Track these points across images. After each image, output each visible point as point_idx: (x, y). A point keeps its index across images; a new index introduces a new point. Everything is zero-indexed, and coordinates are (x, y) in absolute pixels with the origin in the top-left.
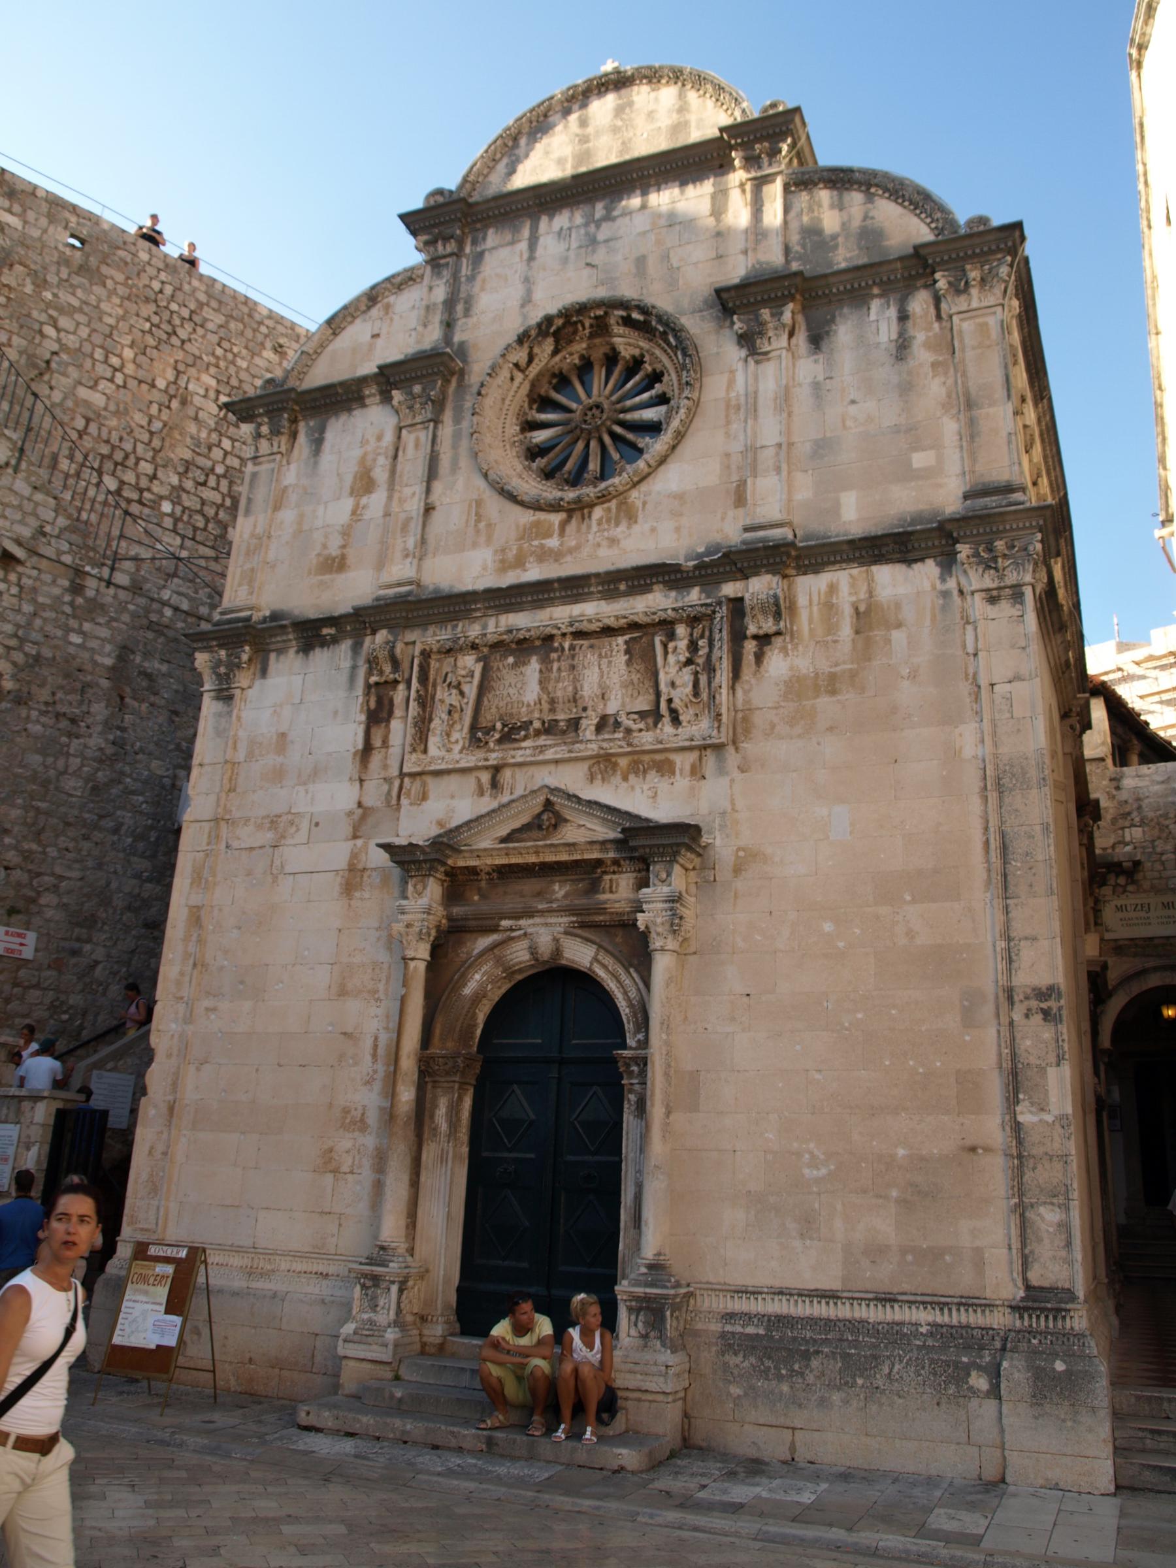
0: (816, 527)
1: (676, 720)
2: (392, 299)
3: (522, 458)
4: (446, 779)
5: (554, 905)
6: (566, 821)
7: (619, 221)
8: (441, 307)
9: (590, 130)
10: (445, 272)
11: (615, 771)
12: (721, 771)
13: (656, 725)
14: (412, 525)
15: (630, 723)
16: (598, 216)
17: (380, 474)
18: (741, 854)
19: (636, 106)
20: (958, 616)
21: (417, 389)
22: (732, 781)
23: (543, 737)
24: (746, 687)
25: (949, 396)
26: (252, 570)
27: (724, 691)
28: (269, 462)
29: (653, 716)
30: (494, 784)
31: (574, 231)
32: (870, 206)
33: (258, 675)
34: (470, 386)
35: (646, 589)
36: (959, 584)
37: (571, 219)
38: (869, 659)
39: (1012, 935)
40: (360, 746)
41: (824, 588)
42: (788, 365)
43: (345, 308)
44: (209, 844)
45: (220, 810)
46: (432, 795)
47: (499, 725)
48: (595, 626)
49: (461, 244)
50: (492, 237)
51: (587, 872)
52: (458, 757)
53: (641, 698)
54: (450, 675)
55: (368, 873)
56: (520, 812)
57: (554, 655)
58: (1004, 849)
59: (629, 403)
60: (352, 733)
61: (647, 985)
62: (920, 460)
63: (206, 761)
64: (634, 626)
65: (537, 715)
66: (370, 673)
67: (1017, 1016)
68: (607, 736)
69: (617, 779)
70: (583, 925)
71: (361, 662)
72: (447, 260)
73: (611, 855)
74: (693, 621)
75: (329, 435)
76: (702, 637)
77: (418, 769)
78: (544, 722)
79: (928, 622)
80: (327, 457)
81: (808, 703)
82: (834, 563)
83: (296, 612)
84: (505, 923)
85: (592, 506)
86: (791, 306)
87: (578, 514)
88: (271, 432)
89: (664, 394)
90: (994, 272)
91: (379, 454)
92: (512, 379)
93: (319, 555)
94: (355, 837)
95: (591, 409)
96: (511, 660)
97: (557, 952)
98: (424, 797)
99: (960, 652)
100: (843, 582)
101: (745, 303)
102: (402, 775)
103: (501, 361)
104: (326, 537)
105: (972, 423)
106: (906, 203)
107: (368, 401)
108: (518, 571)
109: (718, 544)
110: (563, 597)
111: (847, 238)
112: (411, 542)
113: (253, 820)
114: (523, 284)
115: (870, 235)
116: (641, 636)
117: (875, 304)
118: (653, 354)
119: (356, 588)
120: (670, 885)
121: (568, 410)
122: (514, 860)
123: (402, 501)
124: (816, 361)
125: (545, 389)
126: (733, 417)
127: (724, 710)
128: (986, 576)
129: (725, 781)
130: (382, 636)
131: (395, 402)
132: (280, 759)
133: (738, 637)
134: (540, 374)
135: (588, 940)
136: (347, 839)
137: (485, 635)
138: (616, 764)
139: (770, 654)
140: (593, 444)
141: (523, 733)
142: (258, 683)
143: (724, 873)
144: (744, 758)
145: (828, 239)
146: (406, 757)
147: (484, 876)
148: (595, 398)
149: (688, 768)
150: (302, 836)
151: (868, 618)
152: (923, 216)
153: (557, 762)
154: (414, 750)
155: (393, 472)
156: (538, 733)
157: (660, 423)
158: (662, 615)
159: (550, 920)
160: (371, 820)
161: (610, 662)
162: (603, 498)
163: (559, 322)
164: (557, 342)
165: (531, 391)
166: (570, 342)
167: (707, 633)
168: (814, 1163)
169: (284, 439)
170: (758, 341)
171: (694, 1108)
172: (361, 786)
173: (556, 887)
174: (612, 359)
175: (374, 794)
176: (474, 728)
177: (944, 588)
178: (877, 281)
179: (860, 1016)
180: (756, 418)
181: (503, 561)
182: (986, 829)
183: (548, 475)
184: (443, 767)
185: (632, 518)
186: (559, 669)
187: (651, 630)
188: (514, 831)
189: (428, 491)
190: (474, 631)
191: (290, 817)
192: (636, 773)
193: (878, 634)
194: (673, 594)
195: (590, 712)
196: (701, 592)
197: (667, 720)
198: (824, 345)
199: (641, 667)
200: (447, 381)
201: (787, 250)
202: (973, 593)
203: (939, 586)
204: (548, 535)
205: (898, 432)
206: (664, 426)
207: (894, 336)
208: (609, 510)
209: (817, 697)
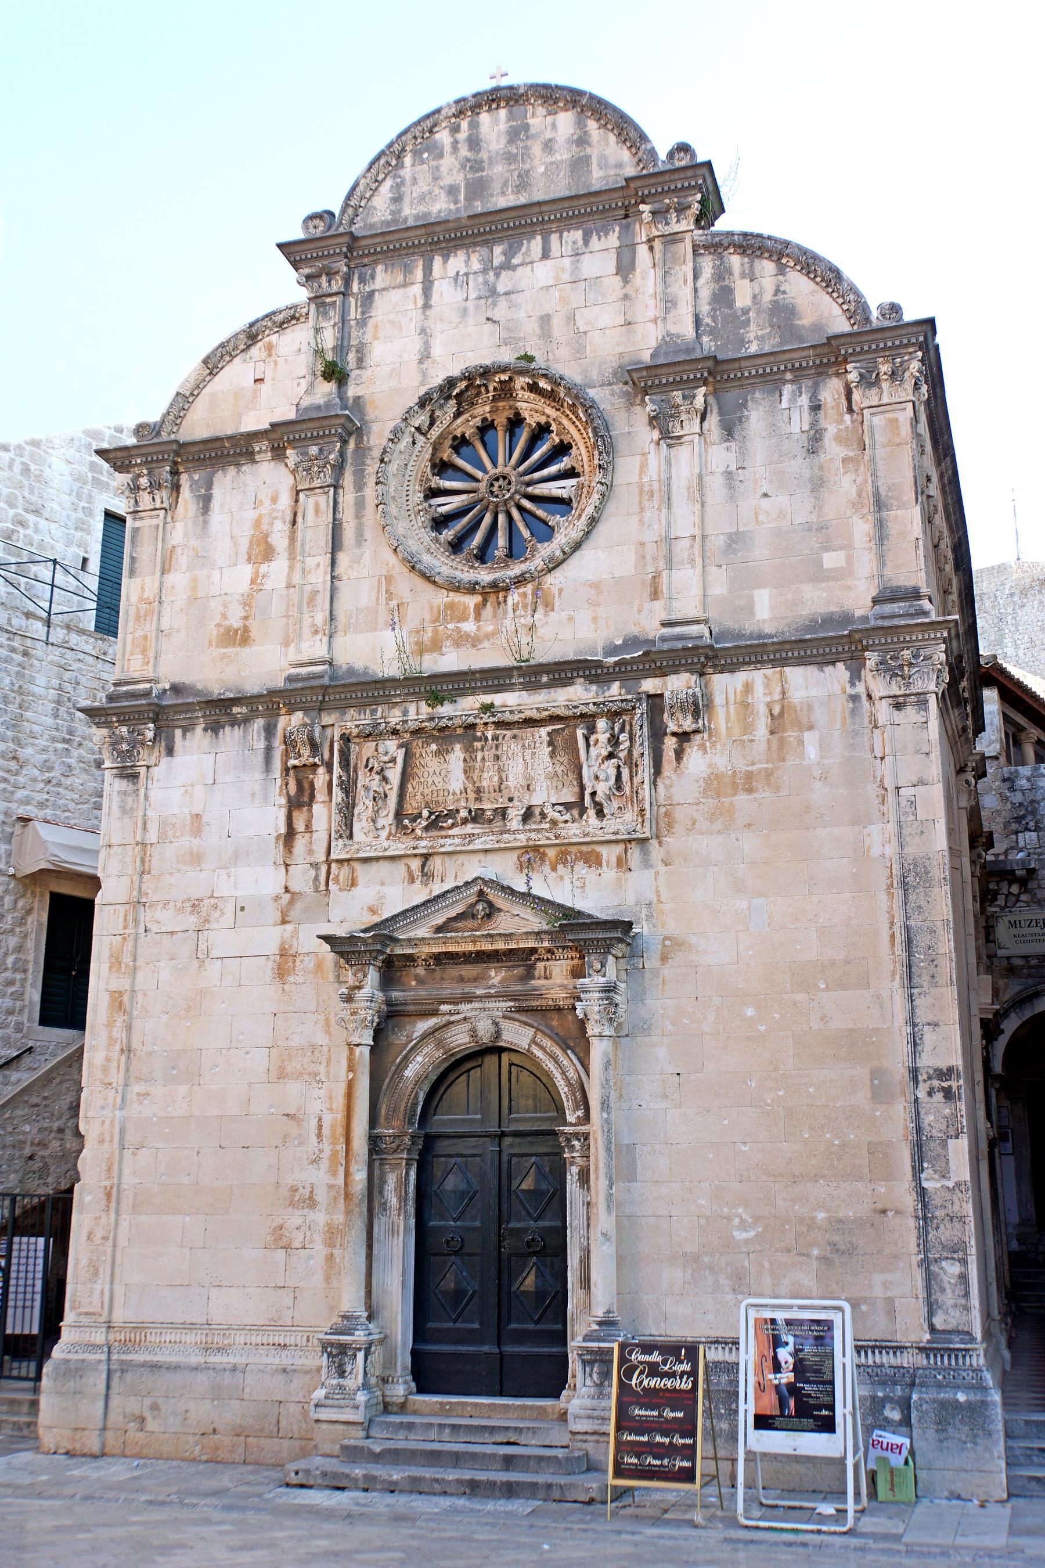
0: (730, 624)
2: (274, 338)
3: (428, 529)
4: (374, 866)
5: (492, 991)
6: (500, 910)
7: (520, 269)
9: (484, 155)
10: (332, 313)
11: (542, 860)
12: (646, 864)
13: (581, 815)
15: (556, 816)
16: (496, 262)
17: (279, 539)
18: (668, 943)
19: (532, 131)
20: (867, 720)
21: (314, 450)
22: (657, 873)
23: (470, 826)
24: (667, 782)
25: (859, 495)
26: (145, 637)
27: (646, 786)
28: (151, 517)
29: (578, 806)
30: (427, 876)
31: (471, 277)
32: (780, 277)
34: (370, 449)
35: (568, 682)
36: (867, 689)
37: (467, 262)
38: (784, 760)
39: (917, 1021)
40: (283, 830)
41: (740, 688)
43: (222, 345)
44: (125, 928)
45: (135, 893)
46: (361, 880)
47: (425, 813)
48: (516, 717)
49: (347, 281)
50: (381, 276)
51: (523, 959)
52: (386, 844)
53: (565, 790)
56: (454, 903)
57: (478, 745)
58: (909, 941)
59: (537, 475)
61: (586, 1067)
62: (831, 560)
63: (114, 841)
64: (554, 719)
65: (463, 804)
66: (286, 755)
67: (921, 1094)
68: (534, 827)
70: (520, 1010)
72: (334, 299)
73: (546, 944)
74: (613, 715)
75: (216, 491)
76: (622, 730)
77: (348, 856)
78: (470, 811)
79: (838, 726)
80: (217, 516)
81: (726, 800)
82: (749, 663)
83: (199, 686)
84: (444, 1008)
85: (507, 589)
86: (703, 389)
87: (492, 598)
89: (573, 468)
90: (905, 365)
91: (276, 518)
92: (414, 443)
93: (218, 625)
94: (284, 922)
95: (497, 479)
96: (434, 747)
98: (353, 883)
99: (869, 756)
100: (758, 680)
101: (655, 381)
102: (328, 862)
103: (403, 425)
104: (225, 606)
105: (881, 525)
106: (818, 279)
107: (257, 458)
108: (435, 654)
109: (636, 637)
111: (758, 312)
112: (321, 617)
113: (172, 903)
114: (421, 335)
115: (782, 313)
116: (566, 729)
117: (788, 389)
118: (560, 423)
119: (264, 666)
120: (604, 976)
121: (477, 480)
122: (452, 948)
125: (447, 454)
126: (647, 503)
127: (647, 806)
128: (893, 683)
129: (649, 873)
130: (298, 717)
131: (291, 462)
132: (197, 841)
133: (657, 734)
134: (442, 437)
135: (526, 1024)
138: (544, 854)
139: (688, 750)
141: (450, 821)
142: (164, 760)
143: (651, 961)
144: (667, 852)
145: (739, 313)
146: (333, 844)
147: (420, 962)
148: (500, 469)
149: (614, 860)
150: (228, 919)
151: (782, 719)
152: (835, 295)
153: (486, 851)
154: (341, 837)
155: (292, 539)
156: (465, 821)
158: (583, 709)
159: (487, 1005)
160: (299, 905)
161: (534, 754)
162: (520, 581)
163: (463, 385)
164: (459, 404)
165: (433, 455)
166: (472, 404)
168: (743, 1226)
169: (165, 493)
170: (671, 424)
171: (632, 1178)
174: (516, 422)
175: (301, 879)
176: (399, 815)
177: (853, 692)
178: (789, 366)
179: (781, 1093)
180: (669, 508)
182: (892, 924)
183: (456, 546)
184: (373, 854)
186: (483, 759)
187: (572, 723)
188: (450, 920)
189: (333, 563)
190: (395, 717)
191: (212, 901)
192: (565, 863)
193: (791, 734)
194: (594, 687)
195: (516, 803)
197: (591, 812)
199: (565, 759)
200: (345, 442)
201: (697, 321)
202: (881, 698)
203: (849, 690)
204: (464, 618)
205: (810, 530)
206: (575, 505)
207: (806, 427)
208: (525, 595)
209: (735, 794)
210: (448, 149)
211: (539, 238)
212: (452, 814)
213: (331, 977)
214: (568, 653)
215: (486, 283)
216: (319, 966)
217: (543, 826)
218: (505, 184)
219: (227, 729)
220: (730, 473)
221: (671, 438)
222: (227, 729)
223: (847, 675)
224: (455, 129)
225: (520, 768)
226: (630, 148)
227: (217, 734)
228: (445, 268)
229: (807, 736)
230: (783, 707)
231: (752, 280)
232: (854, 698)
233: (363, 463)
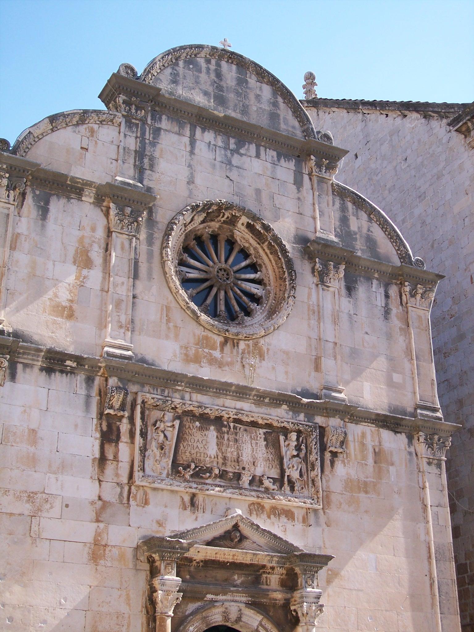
1: (292, 489)
7: (244, 157)
8: (133, 153)
12: (318, 524)
14: (123, 306)
18: (330, 572)
22: (323, 530)
23: (218, 480)
24: (327, 478)
33: (8, 377)
34: (157, 222)
38: (381, 479)
40: (97, 455)
41: (360, 434)
42: (332, 296)
47: (193, 466)
53: (273, 470)
54: (158, 422)
55: (110, 548)
57: (224, 429)
60: (90, 444)
64: (269, 426)
68: (255, 488)
69: (264, 516)
71: (94, 392)
73: (274, 564)
82: (366, 422)
83: (36, 338)
84: (209, 596)
88: (8, 186)
89: (263, 280)
91: (94, 242)
94: (98, 521)
97: (239, 620)
98: (146, 503)
99: (417, 486)
107: (83, 198)
108: (197, 365)
109: (307, 390)
110: (233, 396)
111: (361, 236)
113: (12, 492)
115: (371, 243)
116: (274, 434)
117: (375, 282)
123: (115, 285)
124: (349, 302)
129: (319, 529)
132: (32, 449)
136: (92, 522)
137: (184, 404)
139: (336, 463)
140: (222, 294)
144: (328, 518)
150: (56, 511)
156: (216, 476)
157: (261, 297)
160: (109, 511)
161: (257, 443)
166: (212, 220)
167: (304, 441)
170: (325, 278)
172: (100, 485)
173: (236, 577)
175: (110, 493)
176: (175, 464)
181: (186, 355)
185: (262, 356)
186: (228, 439)
191: (44, 495)
194: (291, 413)
196: (305, 417)
198: (353, 293)
204: (216, 350)
207: (384, 305)
209: (359, 493)
210: (204, 70)
211: (254, 145)
212: (210, 470)
213: (131, 565)
214: (274, 388)
215: (226, 156)
216: (122, 557)
217: (260, 489)
218: (236, 105)
219: (57, 373)
220: (350, 315)
221: (325, 285)
222: (57, 373)
223: (406, 440)
224: (208, 61)
225: (249, 451)
226: (299, 122)
227: (50, 376)
228: (203, 136)
229: (391, 468)
230: (380, 450)
231: (357, 219)
232: (410, 453)
233: (153, 230)
